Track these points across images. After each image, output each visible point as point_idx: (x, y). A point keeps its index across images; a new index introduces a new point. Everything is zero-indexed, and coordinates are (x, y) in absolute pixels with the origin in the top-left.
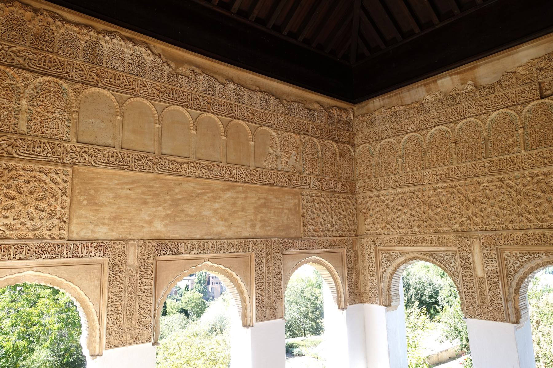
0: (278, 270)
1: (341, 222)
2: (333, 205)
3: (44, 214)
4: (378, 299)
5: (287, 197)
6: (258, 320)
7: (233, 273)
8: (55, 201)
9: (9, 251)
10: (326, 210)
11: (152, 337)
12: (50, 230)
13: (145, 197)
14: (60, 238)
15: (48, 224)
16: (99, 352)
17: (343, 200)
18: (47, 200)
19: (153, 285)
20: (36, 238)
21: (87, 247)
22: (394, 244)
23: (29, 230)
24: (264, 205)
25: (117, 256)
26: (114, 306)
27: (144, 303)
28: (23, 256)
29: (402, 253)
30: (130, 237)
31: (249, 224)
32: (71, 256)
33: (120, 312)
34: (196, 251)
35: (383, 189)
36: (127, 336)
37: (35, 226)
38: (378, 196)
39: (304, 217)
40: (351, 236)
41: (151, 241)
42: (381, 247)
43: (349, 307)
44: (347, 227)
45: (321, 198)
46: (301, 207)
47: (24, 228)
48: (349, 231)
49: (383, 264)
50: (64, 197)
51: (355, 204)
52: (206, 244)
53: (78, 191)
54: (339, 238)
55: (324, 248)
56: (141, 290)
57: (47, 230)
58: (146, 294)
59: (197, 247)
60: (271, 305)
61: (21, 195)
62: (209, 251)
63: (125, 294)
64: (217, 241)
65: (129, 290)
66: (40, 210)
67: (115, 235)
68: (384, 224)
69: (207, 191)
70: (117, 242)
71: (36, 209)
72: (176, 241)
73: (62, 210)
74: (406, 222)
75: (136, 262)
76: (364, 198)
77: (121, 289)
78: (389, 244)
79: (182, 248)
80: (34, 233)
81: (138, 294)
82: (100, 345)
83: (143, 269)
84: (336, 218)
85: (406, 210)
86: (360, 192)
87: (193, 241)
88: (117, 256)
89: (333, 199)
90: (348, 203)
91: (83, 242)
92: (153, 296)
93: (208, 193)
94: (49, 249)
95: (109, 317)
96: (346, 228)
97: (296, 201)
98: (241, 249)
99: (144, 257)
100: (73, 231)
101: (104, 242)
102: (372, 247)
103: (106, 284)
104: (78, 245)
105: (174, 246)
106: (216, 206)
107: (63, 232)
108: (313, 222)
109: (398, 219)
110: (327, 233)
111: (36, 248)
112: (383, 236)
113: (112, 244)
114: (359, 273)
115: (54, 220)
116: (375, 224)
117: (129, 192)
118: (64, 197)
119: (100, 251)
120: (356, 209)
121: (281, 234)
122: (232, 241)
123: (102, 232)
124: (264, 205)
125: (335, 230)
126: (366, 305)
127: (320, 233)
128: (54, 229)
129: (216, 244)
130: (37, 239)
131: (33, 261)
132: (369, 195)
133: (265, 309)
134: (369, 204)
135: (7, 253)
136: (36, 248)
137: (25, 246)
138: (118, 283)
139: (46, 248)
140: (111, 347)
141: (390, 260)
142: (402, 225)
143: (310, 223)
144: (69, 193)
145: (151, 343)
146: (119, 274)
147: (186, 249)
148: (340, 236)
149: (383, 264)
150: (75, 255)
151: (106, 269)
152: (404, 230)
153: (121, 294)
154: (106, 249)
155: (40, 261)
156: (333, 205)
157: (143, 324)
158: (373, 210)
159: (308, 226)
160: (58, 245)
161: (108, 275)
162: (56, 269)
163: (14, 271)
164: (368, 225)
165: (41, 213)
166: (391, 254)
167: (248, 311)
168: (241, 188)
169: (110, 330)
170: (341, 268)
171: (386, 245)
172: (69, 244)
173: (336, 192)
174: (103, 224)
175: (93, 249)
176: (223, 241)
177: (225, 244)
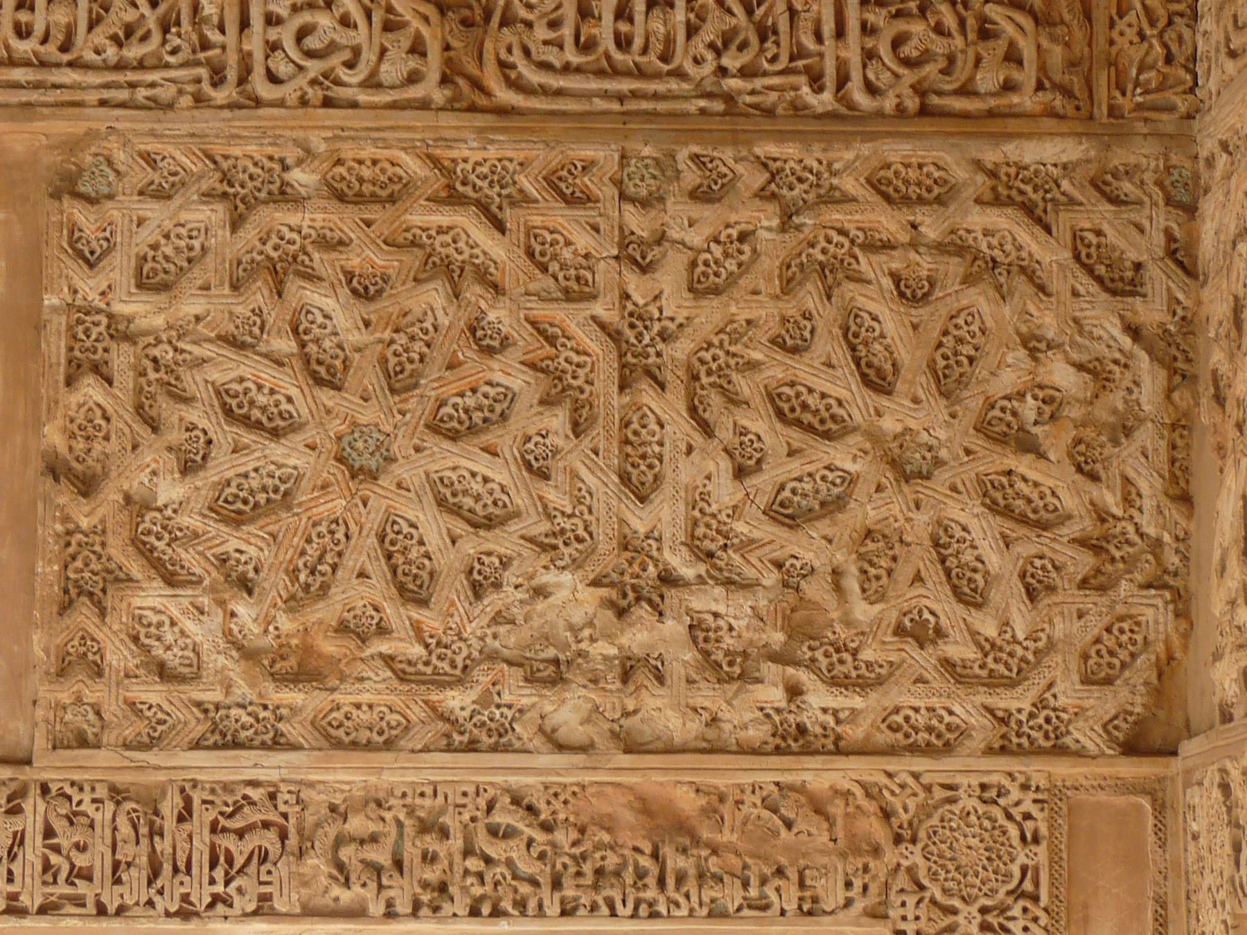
1: (808, 547)
2: (675, 304)
10: (507, 373)
17: (889, 223)
39: (87, 486)
45: (422, 217)
46: (56, 347)
48: (999, 668)
54: (768, 774)
84: (725, 492)
96: (919, 632)
110: (517, 693)
125: (682, 657)
127: (370, 694)
148: (794, 740)
156: (675, 304)
159: (152, 597)
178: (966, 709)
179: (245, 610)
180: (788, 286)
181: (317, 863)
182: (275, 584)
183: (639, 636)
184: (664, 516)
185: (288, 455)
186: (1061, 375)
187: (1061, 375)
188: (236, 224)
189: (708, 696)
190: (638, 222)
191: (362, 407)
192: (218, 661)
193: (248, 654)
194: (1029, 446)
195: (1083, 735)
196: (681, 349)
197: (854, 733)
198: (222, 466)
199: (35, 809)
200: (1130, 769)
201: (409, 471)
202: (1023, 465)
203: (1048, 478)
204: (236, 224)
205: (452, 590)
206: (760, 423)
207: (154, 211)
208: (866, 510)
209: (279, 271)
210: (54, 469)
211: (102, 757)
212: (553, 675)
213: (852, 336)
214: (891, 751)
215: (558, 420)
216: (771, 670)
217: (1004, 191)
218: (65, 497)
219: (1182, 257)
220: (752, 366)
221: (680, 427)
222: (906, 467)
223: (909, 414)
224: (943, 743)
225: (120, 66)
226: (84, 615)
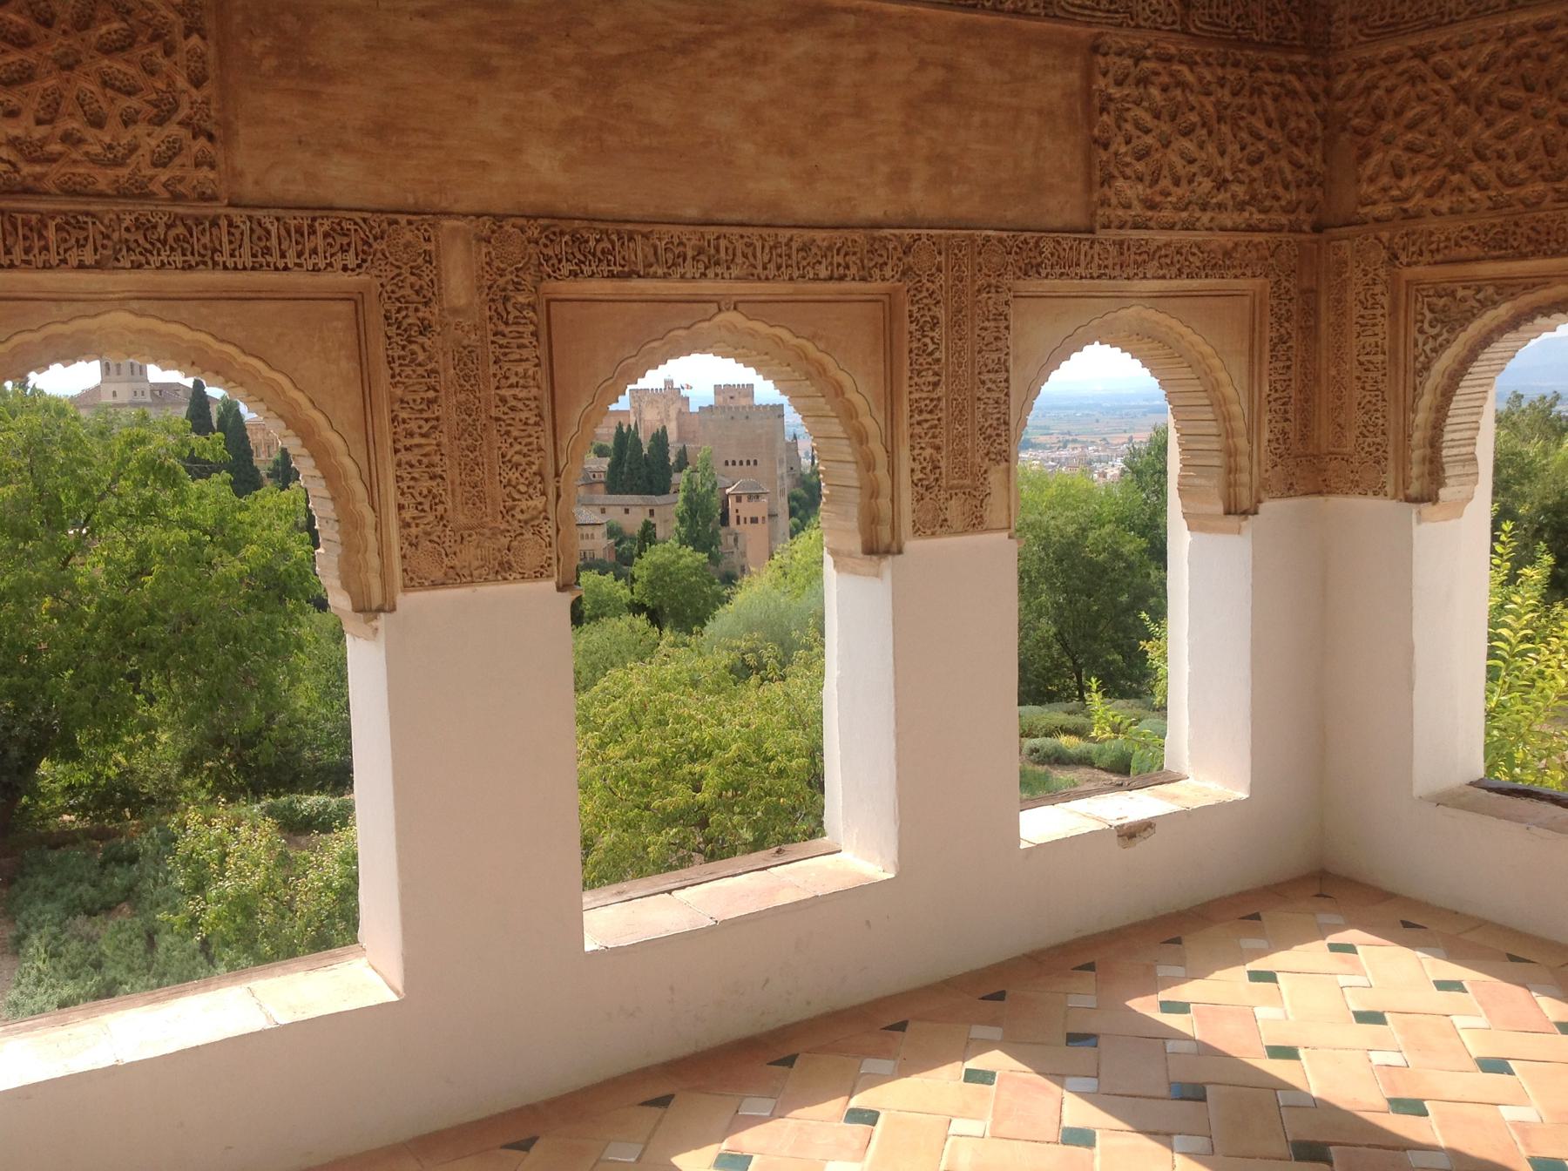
0: (995, 356)
1: (1256, 172)
2: (1227, 99)
3: (134, 102)
4: (1390, 479)
5: (1035, 60)
6: (919, 530)
7: (826, 359)
8: (167, 54)
9: (41, 236)
11: (554, 562)
12: (164, 165)
13: (485, 47)
14: (203, 197)
15: (153, 143)
16: (385, 599)
17: (1270, 76)
18: (139, 52)
19: (545, 385)
20: (122, 194)
21: (299, 231)
22: (1475, 251)
23: (93, 161)
24: (943, 94)
25: (405, 271)
26: (416, 451)
27: (517, 447)
28: (89, 258)
29: (1506, 288)
30: (444, 204)
31: (884, 169)
32: (249, 264)
33: (438, 470)
34: (689, 269)
35: (1446, 19)
36: (469, 555)
37: (110, 147)
38: (1423, 55)
39: (1106, 146)
40: (1295, 229)
41: (522, 222)
42: (1420, 271)
43: (1269, 507)
44: (1279, 190)
45: (1176, 67)
46: (1096, 102)
47: (75, 156)
48: (1291, 209)
49: (1421, 339)
50: (195, 39)
51: (1322, 97)
52: (723, 243)
53: (238, 18)
55: (1180, 273)
56: (503, 400)
57: (155, 165)
58: (523, 415)
59: (690, 253)
60: (968, 482)
61: (43, 31)
62: (735, 272)
63: (447, 409)
64: (765, 232)
65: (462, 397)
66: (119, 90)
67: (388, 192)
68: (1441, 172)
69: (717, 28)
70: (403, 219)
71: (105, 84)
72: (611, 227)
73: (193, 90)
74: (1538, 156)
75: (477, 300)
76: (1364, 66)
77: (431, 394)
78: (1455, 253)
79: (638, 251)
80: (111, 173)
81: (494, 412)
82: (382, 576)
83: (502, 327)
84: (1239, 155)
85: (1542, 102)
86: (1346, 41)
87: (676, 230)
88: (405, 271)
89: (1231, 74)
90: (1292, 94)
91: (281, 213)
92: (548, 425)
93: (720, 35)
94: (172, 233)
95: (403, 485)
96: (1277, 198)
97: (1074, 77)
98: (853, 270)
99: (501, 281)
100: (241, 174)
101: (356, 216)
102: (1382, 272)
103: (385, 373)
104: (267, 223)
105: (606, 245)
106: (756, 90)
107: (205, 172)
108: (1140, 167)
109: (1501, 146)
110: (1197, 214)
111: (127, 229)
112: (1432, 224)
113: (385, 225)
114: (1317, 380)
115: (172, 129)
116: (1399, 176)
117: (421, 25)
118: (195, 39)
119: (344, 250)
120: (1322, 116)
121: (1010, 215)
122: (819, 235)
123: (345, 179)
124: (943, 94)
126: (1335, 501)
127: (1167, 214)
128: (178, 161)
129: (759, 245)
130: (125, 196)
131: (124, 276)
132: (1383, 54)
133: (943, 495)
134: (1380, 92)
135: (37, 244)
136: (127, 229)
137: (89, 220)
138: (420, 370)
139: (161, 230)
140: (421, 585)
141: (1453, 322)
142: (1518, 167)
143: (1128, 171)
144: (210, 24)
145: (550, 585)
146: (421, 339)
147: (652, 259)
148: (1252, 229)
149: (1421, 339)
150: (260, 259)
151: (375, 318)
152: (1524, 192)
153: (437, 411)
154: (366, 243)
155: (147, 277)
156: (1227, 99)
157: (521, 517)
158: (1398, 114)
159: (1120, 183)
160: (198, 221)
161: (383, 339)
162: (204, 311)
163: (67, 309)
164: (1371, 180)
165: (125, 102)
166: (1460, 293)
167: (884, 503)
168: (851, 20)
169: (414, 530)
170: (1245, 359)
171: (1439, 257)
172: (237, 220)
173: (1243, 42)
174: (344, 148)
175: (319, 241)
176: (788, 233)
177: (794, 246)
178: (1284, 220)
179: (1140, 187)
180: (1251, 95)
181: (1156, 263)
182: (1147, 179)
183: (1221, 197)
184: (1227, 160)
185: (1149, 140)
186: (1303, 125)
187: (1303, 125)
188: (1136, 65)
189: (1235, 216)
190: (1220, 72)
191: (1166, 127)
192: (1135, 203)
193: (1141, 201)
194: (1297, 145)
195: (1306, 228)
196: (1229, 112)
197: (1263, 226)
198: (1135, 142)
199: (1097, 246)
200: (1315, 237)
201: (1175, 146)
202: (1295, 150)
203: (1299, 154)
204: (1136, 65)
205: (1184, 182)
206: (1244, 135)
207: (1117, 59)
208: (1266, 162)
209: (1143, 81)
210: (1096, 141)
211: (1112, 231)
212: (1204, 208)
213: (1264, 111)
214: (1270, 231)
215: (1204, 132)
216: (1248, 208)
217: (1295, 70)
218: (1101, 151)
219: (1328, 92)
220: (1242, 118)
221: (1230, 136)
222: (1275, 151)
223: (1275, 135)
224: (1280, 229)
225: (1108, 11)
226: (1106, 187)
